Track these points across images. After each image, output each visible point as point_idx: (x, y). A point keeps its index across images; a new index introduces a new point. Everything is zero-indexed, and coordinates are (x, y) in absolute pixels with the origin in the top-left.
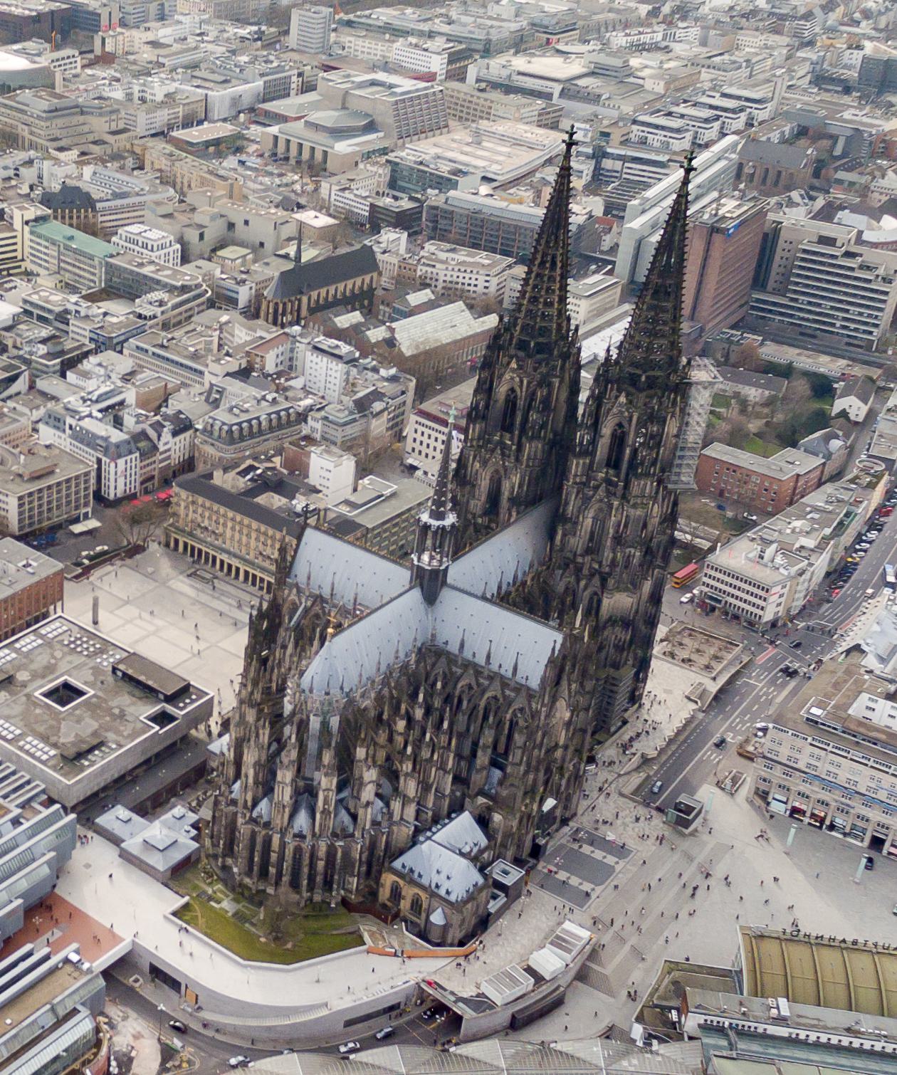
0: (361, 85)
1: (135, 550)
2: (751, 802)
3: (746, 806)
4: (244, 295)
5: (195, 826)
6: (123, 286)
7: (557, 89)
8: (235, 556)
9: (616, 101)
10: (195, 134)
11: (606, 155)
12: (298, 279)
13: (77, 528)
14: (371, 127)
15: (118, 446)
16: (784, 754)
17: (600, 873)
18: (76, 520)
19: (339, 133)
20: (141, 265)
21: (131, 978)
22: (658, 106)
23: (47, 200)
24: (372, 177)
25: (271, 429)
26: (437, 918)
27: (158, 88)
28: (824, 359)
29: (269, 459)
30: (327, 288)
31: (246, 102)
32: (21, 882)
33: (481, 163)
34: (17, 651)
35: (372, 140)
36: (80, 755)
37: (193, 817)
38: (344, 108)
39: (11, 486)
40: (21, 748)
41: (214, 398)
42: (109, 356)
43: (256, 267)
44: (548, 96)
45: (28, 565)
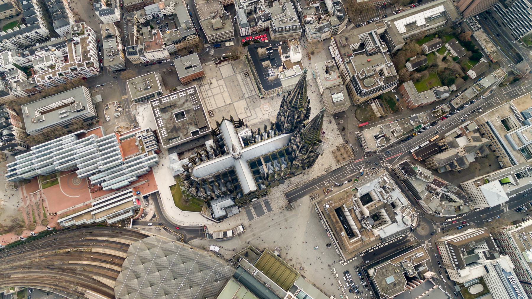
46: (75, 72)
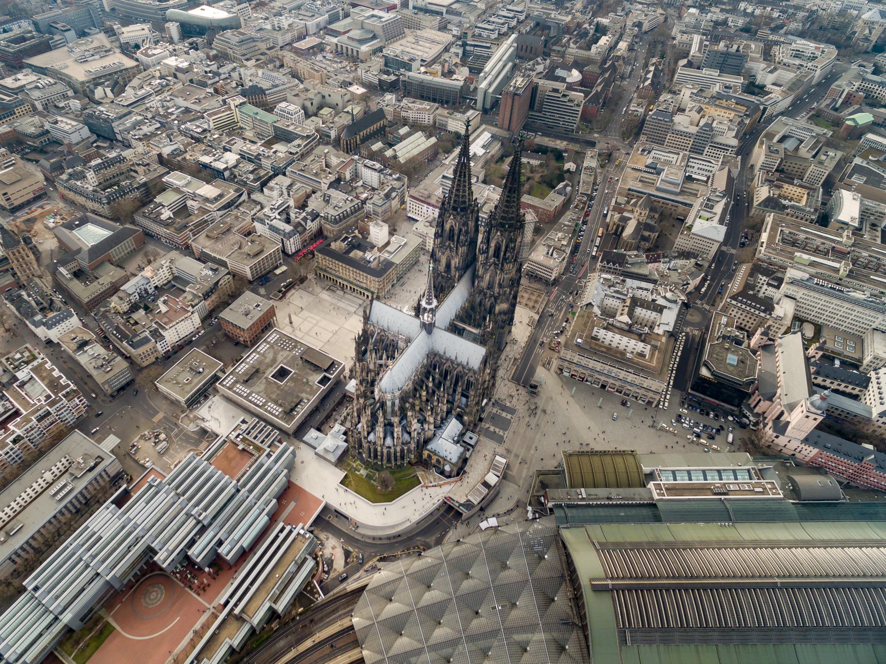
0: (368, 18)
1: (302, 280)
2: (556, 372)
3: (555, 374)
4: (333, 134)
5: (345, 434)
6: (282, 136)
7: (444, 10)
8: (345, 280)
9: (468, 15)
10: (303, 45)
11: (467, 45)
12: (355, 127)
13: (278, 272)
14: (374, 37)
15: (289, 233)
16: (568, 358)
17: (505, 425)
18: (277, 267)
19: (362, 42)
20: (288, 126)
21: (328, 520)
22: (484, 17)
23: (244, 94)
24: (377, 62)
25: (352, 213)
26: (447, 468)
27: (285, 21)
28: (558, 142)
29: (353, 232)
30: (367, 133)
31: (322, 25)
32: (275, 488)
33: (420, 53)
34: (258, 353)
35: (375, 43)
36: (292, 410)
37: (343, 429)
38: (363, 28)
39: (245, 262)
40: (266, 410)
41: (327, 200)
42: (280, 178)
43: (336, 119)
44: (441, 14)
45: (258, 306)
46: (46, 422)
